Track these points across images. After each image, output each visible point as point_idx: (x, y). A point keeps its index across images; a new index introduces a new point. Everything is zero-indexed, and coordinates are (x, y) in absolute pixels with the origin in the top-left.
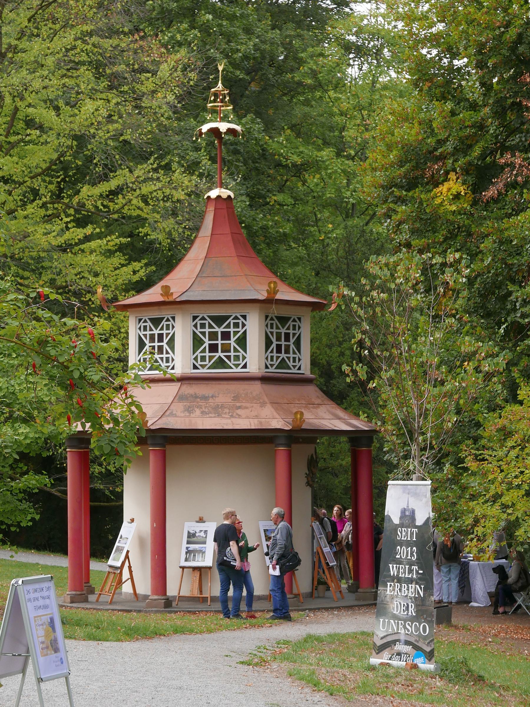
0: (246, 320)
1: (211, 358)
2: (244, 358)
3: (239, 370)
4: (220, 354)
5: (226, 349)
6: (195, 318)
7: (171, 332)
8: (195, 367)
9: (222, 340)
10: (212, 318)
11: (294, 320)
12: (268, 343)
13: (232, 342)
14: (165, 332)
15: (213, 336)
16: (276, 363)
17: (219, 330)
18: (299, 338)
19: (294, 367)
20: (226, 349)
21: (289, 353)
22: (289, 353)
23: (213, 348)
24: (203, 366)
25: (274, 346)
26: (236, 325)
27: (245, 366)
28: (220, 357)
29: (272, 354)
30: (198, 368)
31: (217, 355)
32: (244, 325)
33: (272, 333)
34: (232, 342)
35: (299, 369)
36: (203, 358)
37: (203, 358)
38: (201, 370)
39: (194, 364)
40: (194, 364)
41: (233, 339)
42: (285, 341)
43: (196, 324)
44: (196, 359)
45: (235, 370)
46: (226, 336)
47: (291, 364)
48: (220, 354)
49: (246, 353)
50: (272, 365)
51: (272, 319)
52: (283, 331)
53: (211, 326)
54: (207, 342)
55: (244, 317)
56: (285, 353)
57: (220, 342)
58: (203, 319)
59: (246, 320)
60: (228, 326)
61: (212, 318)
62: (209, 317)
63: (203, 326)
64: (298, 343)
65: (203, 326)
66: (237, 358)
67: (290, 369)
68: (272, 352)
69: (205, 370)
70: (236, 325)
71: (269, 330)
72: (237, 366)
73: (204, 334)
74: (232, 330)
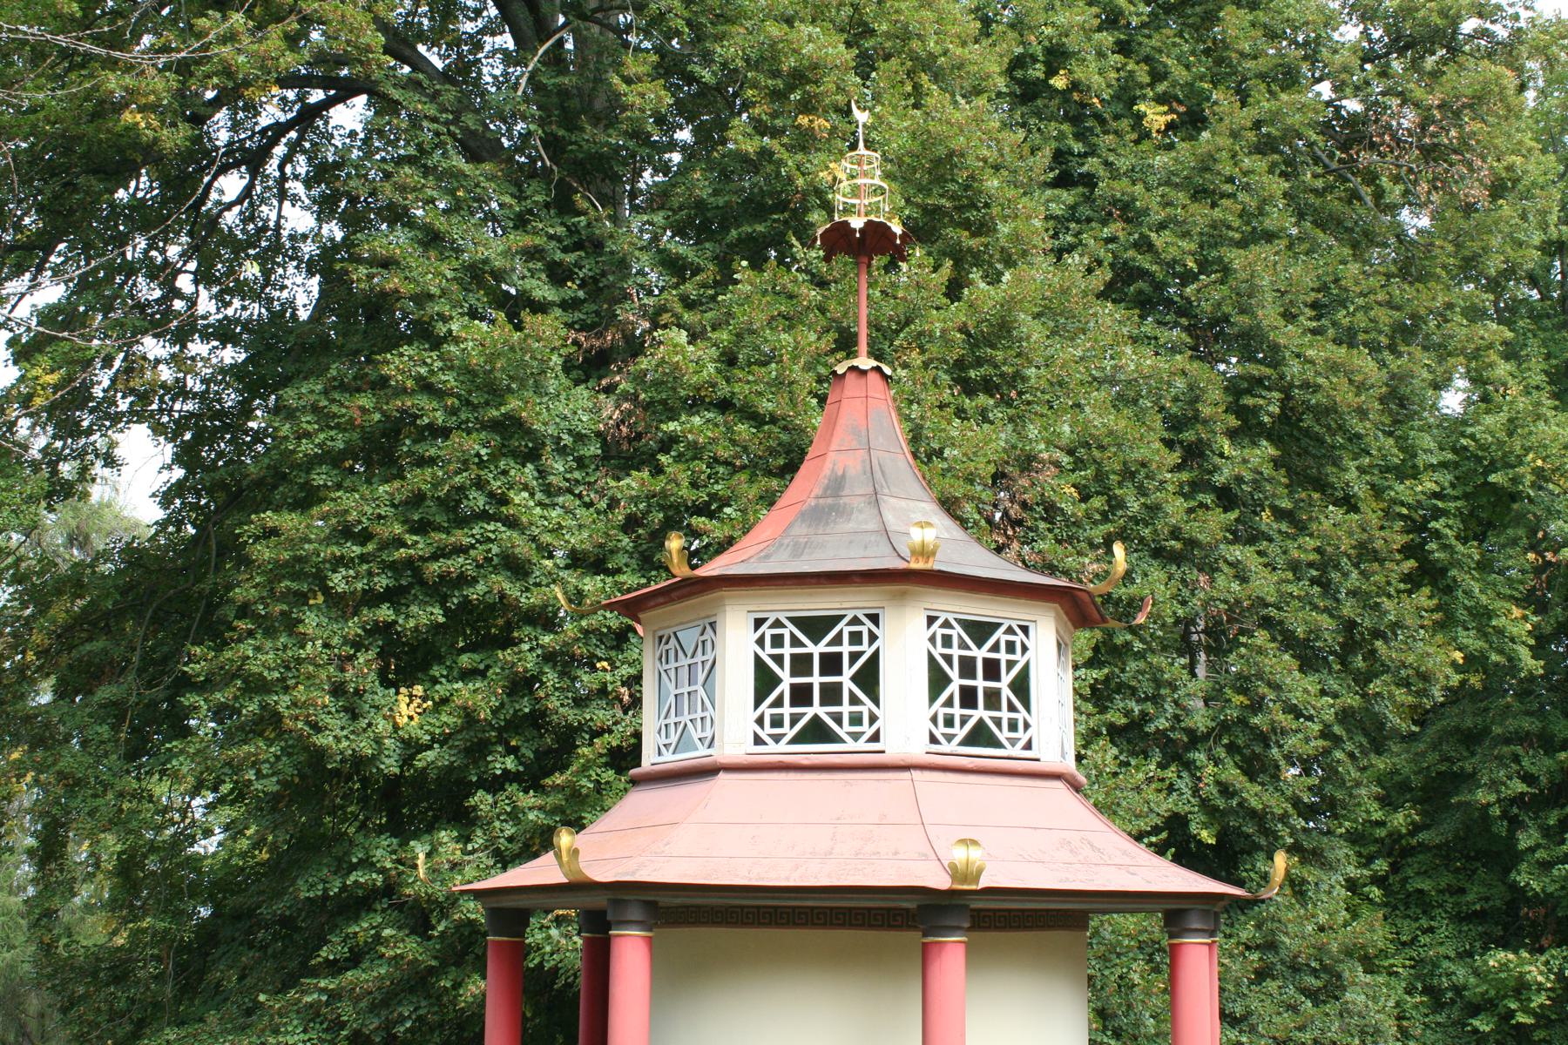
0: (877, 624)
1: (795, 719)
2: (873, 719)
3: (861, 745)
4: (817, 709)
5: (831, 695)
6: (759, 623)
7: (709, 657)
8: (758, 741)
9: (822, 673)
10: (798, 622)
11: (1010, 631)
12: (938, 681)
13: (846, 679)
14: (699, 658)
15: (801, 664)
16: (961, 733)
17: (816, 650)
18: (1025, 673)
19: (1013, 742)
20: (831, 695)
21: (999, 709)
22: (999, 709)
23: (801, 695)
24: (777, 738)
25: (954, 688)
26: (856, 638)
27: (875, 738)
28: (816, 718)
29: (948, 710)
30: (765, 743)
31: (809, 712)
32: (873, 638)
33: (948, 659)
34: (846, 679)
35: (1028, 746)
36: (777, 722)
37: (777, 722)
38: (772, 747)
39: (756, 736)
40: (756, 736)
41: (848, 672)
42: (986, 678)
43: (762, 637)
44: (760, 721)
45: (851, 745)
46: (831, 664)
47: (1003, 735)
48: (817, 709)
49: (877, 704)
50: (949, 738)
51: (946, 624)
52: (980, 654)
53: (795, 642)
54: (787, 680)
55: (874, 619)
56: (988, 707)
57: (816, 680)
58: (778, 624)
59: (877, 624)
60: (837, 640)
61: (798, 622)
62: (793, 620)
63: (777, 641)
64: (1021, 687)
65: (777, 641)
66: (856, 720)
67: (998, 745)
68: (949, 703)
69: (783, 746)
70: (856, 638)
71: (939, 651)
72: (856, 736)
73: (778, 659)
74: (846, 649)
